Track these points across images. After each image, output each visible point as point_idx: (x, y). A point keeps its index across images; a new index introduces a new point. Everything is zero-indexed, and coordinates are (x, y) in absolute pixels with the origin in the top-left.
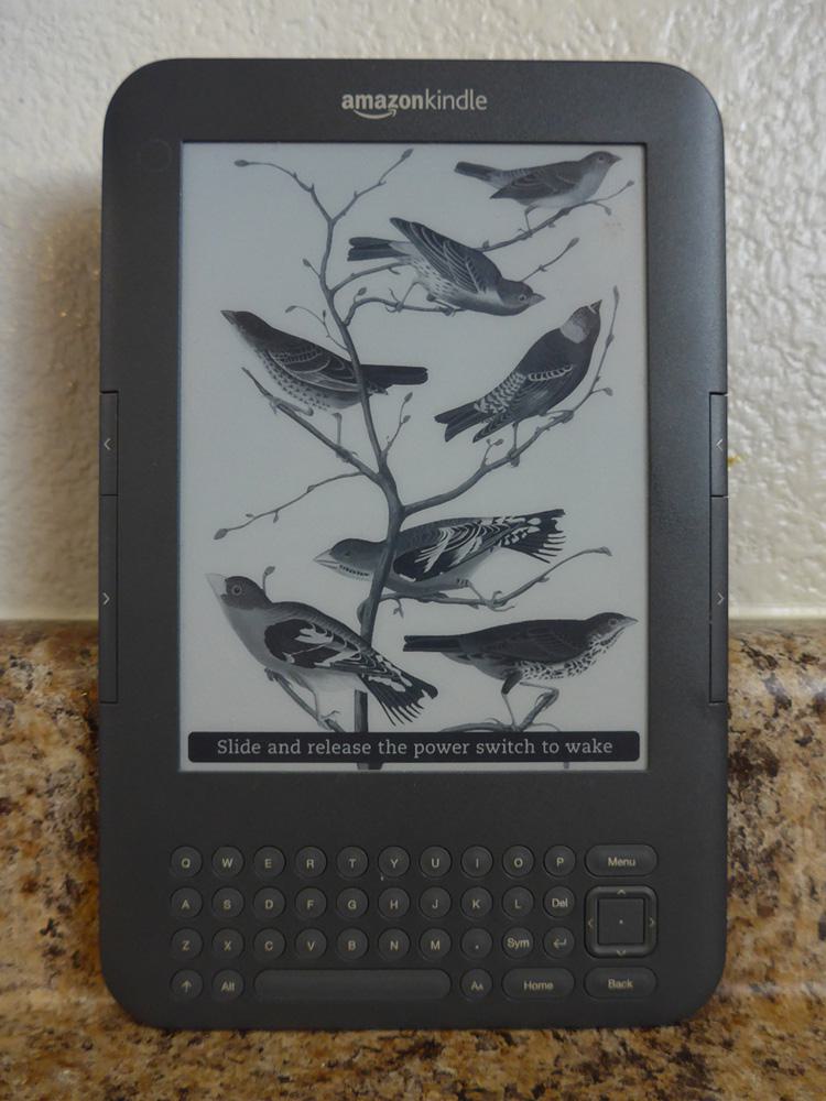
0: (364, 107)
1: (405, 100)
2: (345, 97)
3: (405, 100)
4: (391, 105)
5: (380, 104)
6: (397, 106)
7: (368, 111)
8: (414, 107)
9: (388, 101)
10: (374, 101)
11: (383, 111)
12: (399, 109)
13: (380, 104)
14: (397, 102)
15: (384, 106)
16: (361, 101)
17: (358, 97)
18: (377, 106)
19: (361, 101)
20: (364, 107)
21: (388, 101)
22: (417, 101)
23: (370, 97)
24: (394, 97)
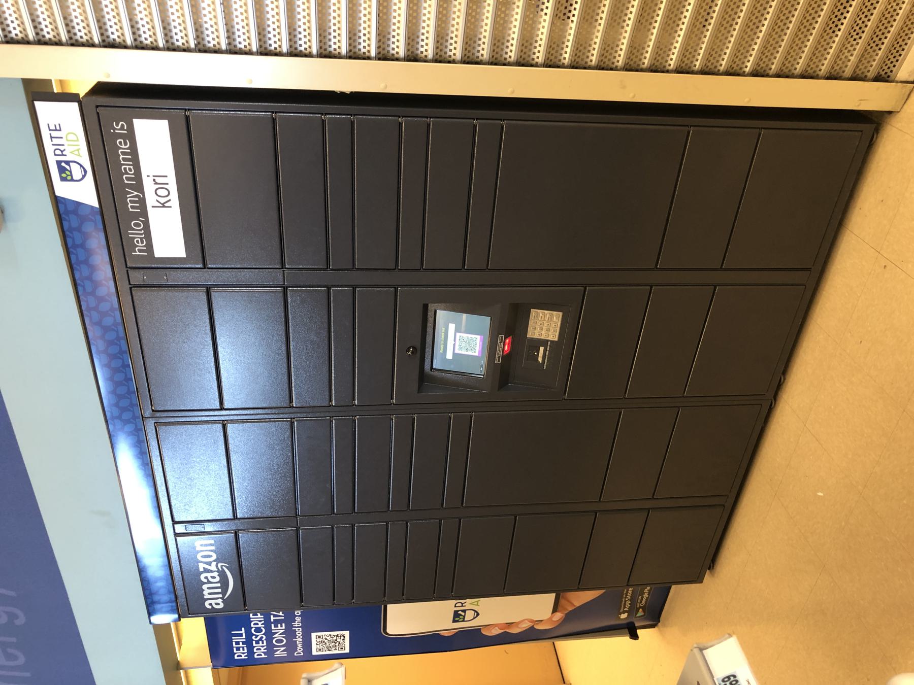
0: (219, 590)
1: (210, 556)
3: (210, 556)
5: (213, 577)
8: (213, 548)
10: (209, 582)
12: (217, 561)
15: (216, 574)
16: (210, 594)
18: (218, 579)
19: (210, 594)
20: (219, 590)
23: (205, 587)
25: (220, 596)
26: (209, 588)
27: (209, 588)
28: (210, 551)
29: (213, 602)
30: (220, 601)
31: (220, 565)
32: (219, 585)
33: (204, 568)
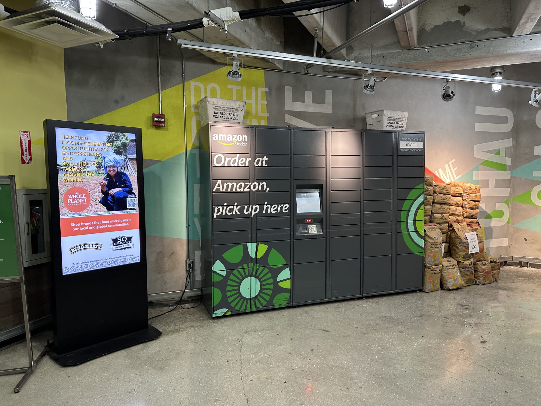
0: (223, 140)
1: (240, 139)
2: (214, 135)
3: (240, 139)
4: (234, 139)
6: (236, 140)
7: (224, 142)
9: (233, 137)
11: (232, 142)
13: (229, 139)
14: (236, 138)
15: (231, 140)
16: (221, 137)
17: (220, 135)
18: (228, 140)
19: (221, 137)
20: (223, 140)
21: (233, 137)
22: (245, 137)
24: (235, 136)
25: (220, 139)
26: (224, 137)
27: (224, 137)
28: (242, 139)
29: (217, 137)
30: (217, 139)
31: (236, 142)
32: (225, 140)
33: (234, 137)
